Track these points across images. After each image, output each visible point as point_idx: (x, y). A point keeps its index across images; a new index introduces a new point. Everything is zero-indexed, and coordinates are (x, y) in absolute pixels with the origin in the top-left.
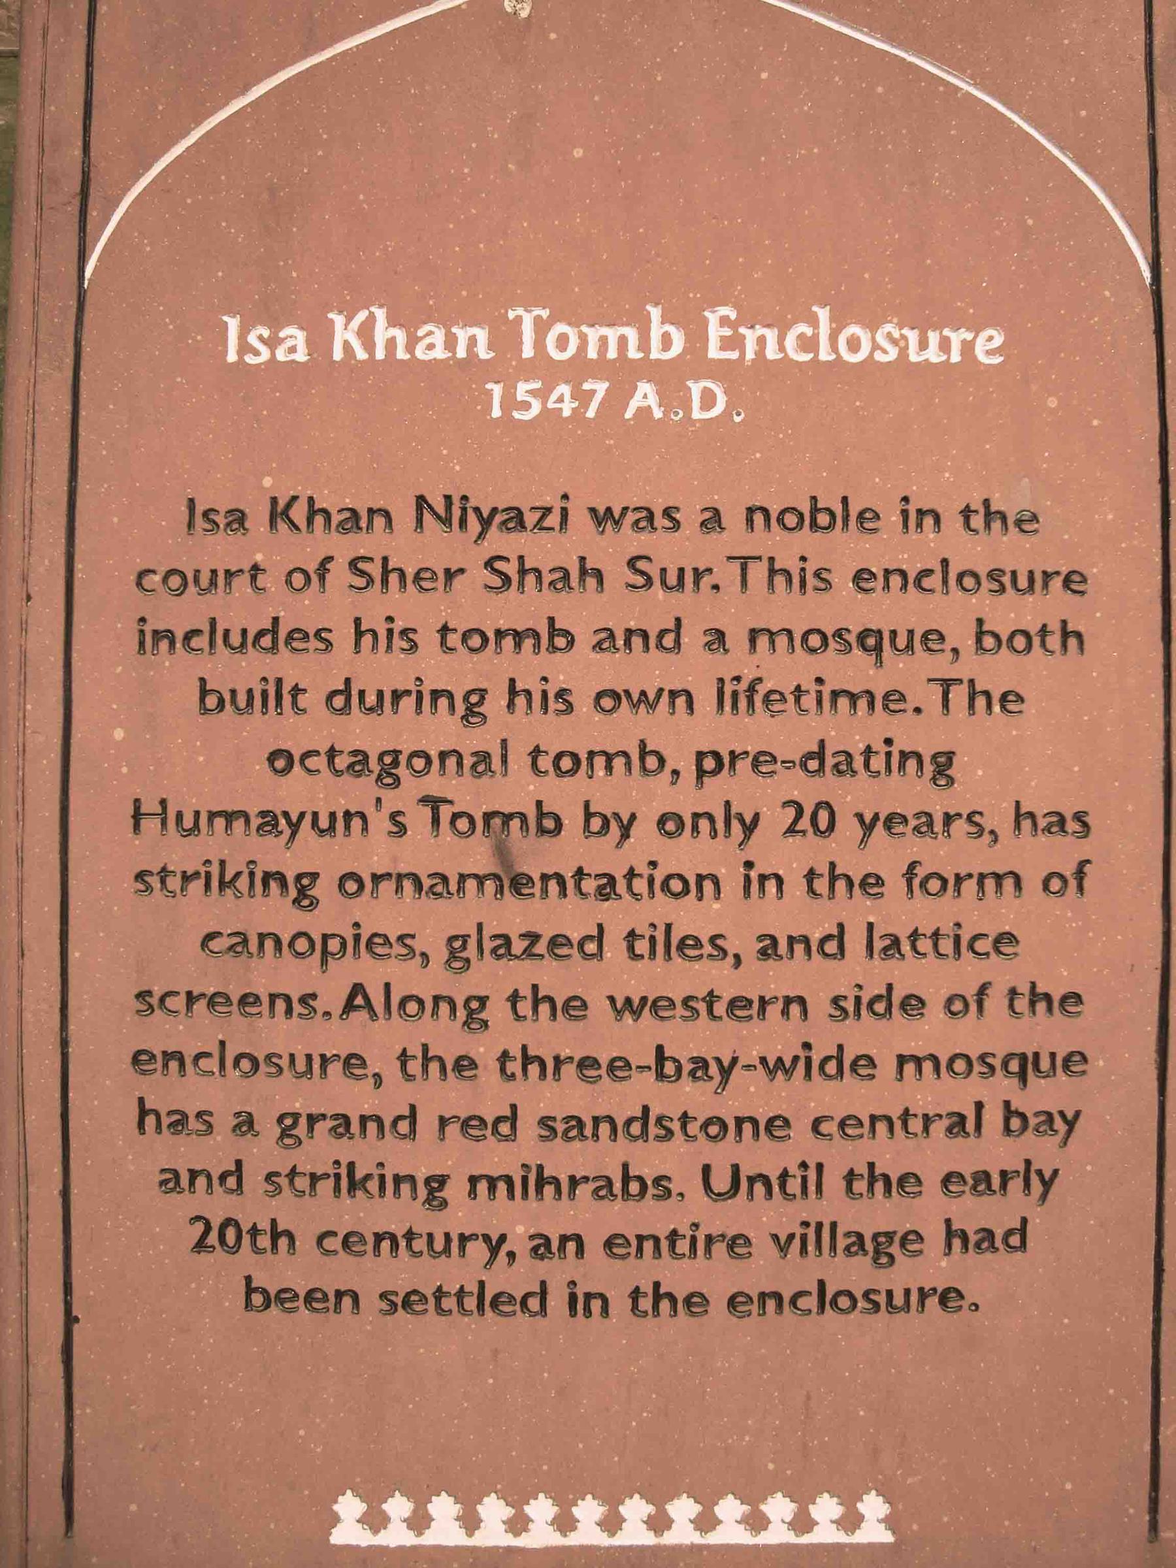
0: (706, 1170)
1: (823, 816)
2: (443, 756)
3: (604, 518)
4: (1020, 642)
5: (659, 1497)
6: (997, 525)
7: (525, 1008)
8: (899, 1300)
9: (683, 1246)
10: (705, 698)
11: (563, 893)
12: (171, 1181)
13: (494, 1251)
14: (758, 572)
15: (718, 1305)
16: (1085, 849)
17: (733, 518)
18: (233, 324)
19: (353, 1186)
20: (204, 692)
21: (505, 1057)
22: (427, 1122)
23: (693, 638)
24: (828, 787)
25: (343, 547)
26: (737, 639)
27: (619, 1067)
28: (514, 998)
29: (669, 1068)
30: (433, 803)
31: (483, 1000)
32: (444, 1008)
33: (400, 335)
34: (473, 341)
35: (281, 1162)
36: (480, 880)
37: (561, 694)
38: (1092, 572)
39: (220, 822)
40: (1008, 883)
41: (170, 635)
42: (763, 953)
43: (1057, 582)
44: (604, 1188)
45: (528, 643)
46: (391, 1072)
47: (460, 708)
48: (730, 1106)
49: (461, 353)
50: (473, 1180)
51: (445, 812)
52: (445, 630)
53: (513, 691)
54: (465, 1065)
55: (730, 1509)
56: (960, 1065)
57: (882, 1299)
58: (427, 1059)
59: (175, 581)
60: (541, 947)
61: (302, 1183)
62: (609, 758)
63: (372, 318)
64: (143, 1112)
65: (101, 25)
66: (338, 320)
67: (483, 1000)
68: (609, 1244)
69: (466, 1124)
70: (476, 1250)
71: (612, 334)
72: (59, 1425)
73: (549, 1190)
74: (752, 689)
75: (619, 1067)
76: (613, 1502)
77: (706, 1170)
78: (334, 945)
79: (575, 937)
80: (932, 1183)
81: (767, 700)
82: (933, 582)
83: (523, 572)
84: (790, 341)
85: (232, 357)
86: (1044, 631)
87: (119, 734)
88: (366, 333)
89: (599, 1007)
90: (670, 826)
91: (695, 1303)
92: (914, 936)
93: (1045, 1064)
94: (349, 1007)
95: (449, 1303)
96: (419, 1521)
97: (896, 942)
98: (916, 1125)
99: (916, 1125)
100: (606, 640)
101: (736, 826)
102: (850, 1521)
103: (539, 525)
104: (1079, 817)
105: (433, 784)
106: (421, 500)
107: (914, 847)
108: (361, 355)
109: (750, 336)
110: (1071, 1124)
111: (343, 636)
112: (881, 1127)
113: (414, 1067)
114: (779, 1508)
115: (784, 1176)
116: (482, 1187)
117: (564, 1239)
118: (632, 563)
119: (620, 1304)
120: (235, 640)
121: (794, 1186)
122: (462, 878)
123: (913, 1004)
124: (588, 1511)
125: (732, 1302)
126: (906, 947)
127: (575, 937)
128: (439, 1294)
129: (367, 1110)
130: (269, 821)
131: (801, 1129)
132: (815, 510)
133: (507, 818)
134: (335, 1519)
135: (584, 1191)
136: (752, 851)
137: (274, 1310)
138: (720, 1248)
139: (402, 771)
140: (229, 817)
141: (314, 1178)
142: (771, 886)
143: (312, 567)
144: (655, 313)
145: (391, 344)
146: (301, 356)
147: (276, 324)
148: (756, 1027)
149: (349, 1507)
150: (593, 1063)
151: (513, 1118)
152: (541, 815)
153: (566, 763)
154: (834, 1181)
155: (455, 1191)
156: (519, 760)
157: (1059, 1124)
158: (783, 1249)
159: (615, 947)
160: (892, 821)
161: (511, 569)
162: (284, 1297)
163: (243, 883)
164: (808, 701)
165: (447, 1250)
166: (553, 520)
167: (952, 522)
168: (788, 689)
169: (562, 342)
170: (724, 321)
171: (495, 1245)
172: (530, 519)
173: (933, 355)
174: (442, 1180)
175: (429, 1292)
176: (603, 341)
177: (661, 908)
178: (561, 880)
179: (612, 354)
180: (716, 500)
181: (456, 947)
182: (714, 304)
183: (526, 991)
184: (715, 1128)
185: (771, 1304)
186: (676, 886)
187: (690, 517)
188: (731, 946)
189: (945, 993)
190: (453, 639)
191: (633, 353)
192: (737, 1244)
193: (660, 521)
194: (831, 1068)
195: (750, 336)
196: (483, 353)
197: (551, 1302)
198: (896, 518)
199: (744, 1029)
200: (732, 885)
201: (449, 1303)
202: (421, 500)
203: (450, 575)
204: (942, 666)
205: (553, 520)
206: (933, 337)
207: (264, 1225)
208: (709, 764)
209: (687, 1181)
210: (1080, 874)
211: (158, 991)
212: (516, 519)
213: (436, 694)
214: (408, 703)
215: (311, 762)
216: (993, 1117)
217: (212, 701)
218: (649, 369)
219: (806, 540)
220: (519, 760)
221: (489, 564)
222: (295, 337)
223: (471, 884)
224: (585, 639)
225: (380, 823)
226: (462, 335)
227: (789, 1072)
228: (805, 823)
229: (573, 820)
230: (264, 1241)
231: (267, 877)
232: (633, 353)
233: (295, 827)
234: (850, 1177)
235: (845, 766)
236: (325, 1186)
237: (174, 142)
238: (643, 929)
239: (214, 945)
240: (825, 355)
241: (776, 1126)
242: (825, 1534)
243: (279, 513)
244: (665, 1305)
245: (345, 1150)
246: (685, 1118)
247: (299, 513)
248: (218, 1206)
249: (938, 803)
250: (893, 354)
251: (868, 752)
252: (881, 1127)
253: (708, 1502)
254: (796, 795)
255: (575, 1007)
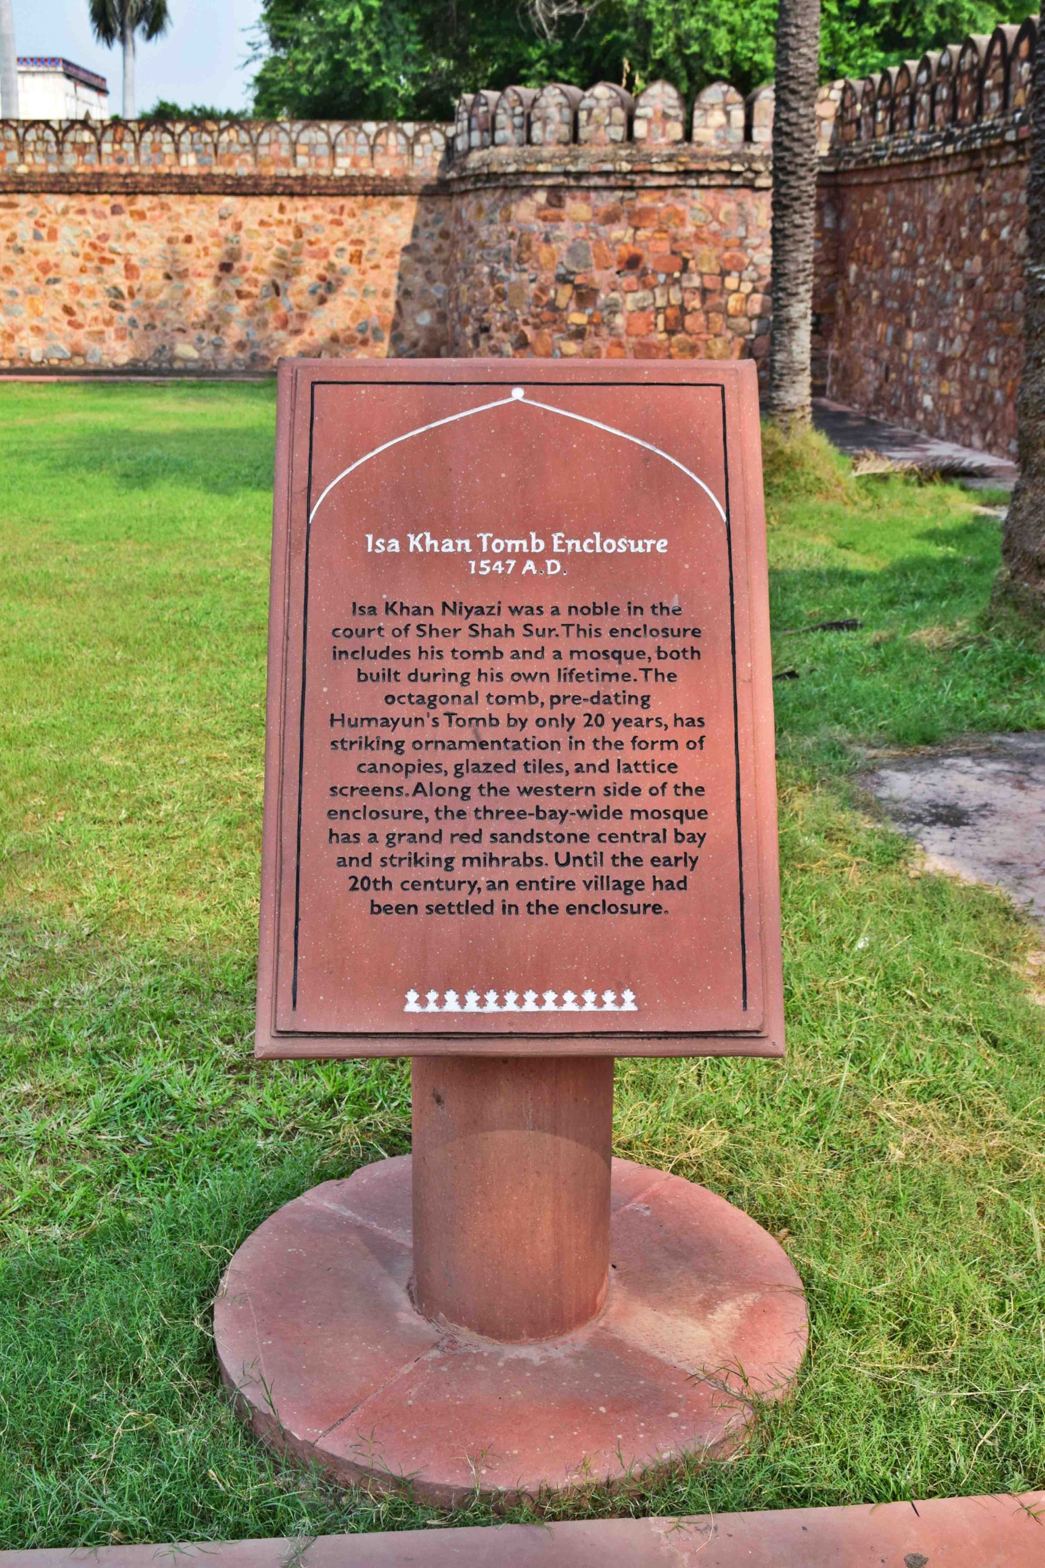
0: (557, 854)
1: (600, 719)
2: (453, 697)
3: (515, 611)
4: (675, 655)
5: (540, 990)
6: (665, 612)
7: (485, 791)
8: (635, 909)
9: (548, 885)
10: (554, 676)
11: (500, 748)
12: (342, 862)
13: (472, 887)
14: (573, 630)
15: (562, 910)
16: (702, 731)
17: (564, 611)
18: (370, 537)
19: (416, 862)
20: (360, 674)
21: (477, 811)
22: (446, 837)
23: (548, 654)
24: (601, 708)
25: (414, 621)
26: (565, 654)
27: (522, 814)
28: (481, 787)
29: (541, 814)
30: (450, 715)
31: (469, 789)
32: (453, 791)
33: (436, 543)
34: (463, 546)
35: (388, 853)
36: (468, 743)
37: (498, 675)
38: (703, 629)
39: (366, 722)
40: (673, 745)
41: (346, 652)
42: (577, 771)
43: (689, 633)
44: (516, 862)
45: (486, 655)
46: (432, 816)
47: (460, 679)
48: (565, 829)
49: (459, 549)
50: (464, 859)
51: (454, 718)
52: (454, 651)
53: (480, 674)
54: (461, 814)
55: (569, 996)
56: (656, 814)
57: (628, 908)
58: (446, 812)
59: (348, 633)
60: (491, 768)
61: (396, 861)
62: (517, 698)
63: (424, 537)
64: (331, 834)
65: (315, 424)
66: (411, 536)
67: (469, 789)
68: (518, 884)
69: (461, 837)
70: (466, 887)
71: (517, 543)
72: (291, 963)
73: (494, 862)
74: (571, 673)
75: (522, 814)
76: (521, 992)
77: (557, 854)
78: (410, 768)
79: (504, 764)
80: (647, 861)
81: (577, 677)
82: (641, 633)
83: (483, 630)
84: (585, 546)
85: (370, 550)
86: (684, 651)
87: (325, 690)
88: (422, 541)
89: (514, 790)
90: (541, 723)
91: (553, 909)
92: (636, 764)
93: (690, 815)
94: (416, 791)
95: (454, 909)
96: (441, 1002)
97: (629, 766)
98: (639, 838)
99: (639, 838)
100: (515, 655)
101: (566, 723)
102: (620, 1002)
103: (489, 614)
104: (700, 720)
105: (450, 708)
106: (445, 605)
107: (634, 730)
108: (421, 550)
109: (570, 543)
110: (702, 839)
111: (414, 653)
112: (625, 838)
113: (441, 815)
114: (589, 996)
115: (588, 857)
116: (468, 861)
117: (500, 883)
118: (525, 626)
119: (523, 909)
120: (372, 654)
121: (591, 861)
122: (461, 742)
123: (636, 791)
124: (511, 997)
125: (568, 908)
126: (633, 768)
127: (504, 764)
128: (450, 905)
129: (422, 831)
130: (386, 722)
131: (593, 839)
132: (595, 607)
133: (478, 720)
134: (406, 1001)
135: (508, 863)
136: (572, 733)
137: (383, 914)
138: (562, 886)
139: (437, 703)
140: (369, 720)
141: (401, 860)
142: (580, 746)
143: (402, 628)
144: (533, 535)
145: (432, 546)
146: (397, 550)
147: (387, 539)
148: (575, 798)
149: (412, 996)
150: (513, 813)
151: (480, 834)
152: (491, 719)
153: (500, 700)
154: (607, 859)
155: (457, 863)
156: (482, 699)
157: (697, 838)
158: (588, 887)
159: (520, 769)
160: (627, 721)
161: (479, 629)
162: (387, 909)
163: (374, 745)
164: (593, 677)
165: (453, 888)
166: (495, 611)
167: (648, 611)
168: (585, 672)
169: (498, 546)
170: (560, 538)
171: (473, 885)
172: (486, 610)
173: (640, 549)
174: (452, 859)
175: (446, 905)
176: (514, 546)
177: (536, 754)
178: (499, 743)
179: (517, 550)
180: (557, 604)
181: (458, 768)
182: (556, 531)
183: (485, 785)
184: (560, 838)
185: (584, 909)
186: (543, 745)
187: (547, 609)
188: (565, 767)
189: (649, 786)
190: (457, 654)
191: (525, 550)
192: (569, 885)
193: (536, 611)
194: (605, 814)
195: (570, 543)
196: (468, 550)
197: (495, 909)
198: (626, 610)
199: (570, 799)
200: (565, 746)
201: (454, 909)
202: (445, 605)
203: (455, 631)
204: (645, 664)
205: (495, 611)
206: (640, 543)
207: (380, 879)
208: (555, 700)
209: (548, 859)
210: (701, 741)
211: (339, 786)
212: (481, 610)
213: (450, 674)
214: (439, 678)
215: (402, 700)
216: (670, 834)
217: (362, 677)
218: (531, 556)
219: (591, 619)
220: (482, 699)
221: (471, 627)
222: (395, 545)
223: (464, 745)
224: (507, 654)
225: (429, 722)
226: (459, 542)
227: (588, 816)
228: (592, 722)
229: (503, 721)
230: (379, 886)
231: (384, 742)
232: (525, 550)
233: (395, 724)
234: (614, 858)
235: (608, 700)
236: (405, 863)
237: (344, 469)
238: (530, 761)
239: (363, 769)
240: (598, 550)
241: (584, 837)
242: (610, 1007)
243: (389, 608)
244: (541, 909)
245: (413, 848)
246: (548, 834)
247: (397, 608)
248: (361, 872)
249: (644, 715)
250: (624, 549)
251: (616, 696)
252: (625, 838)
253: (560, 993)
254: (589, 711)
255: (504, 791)
